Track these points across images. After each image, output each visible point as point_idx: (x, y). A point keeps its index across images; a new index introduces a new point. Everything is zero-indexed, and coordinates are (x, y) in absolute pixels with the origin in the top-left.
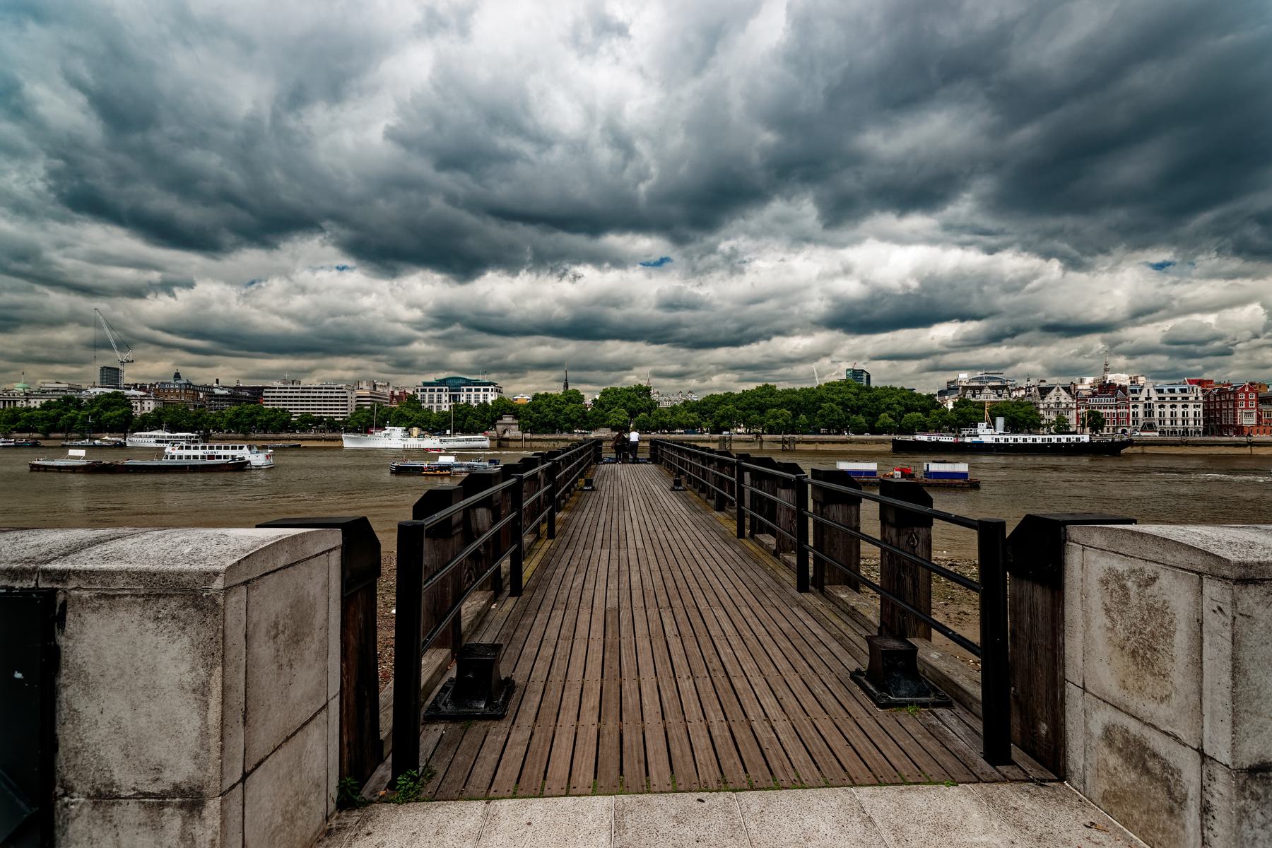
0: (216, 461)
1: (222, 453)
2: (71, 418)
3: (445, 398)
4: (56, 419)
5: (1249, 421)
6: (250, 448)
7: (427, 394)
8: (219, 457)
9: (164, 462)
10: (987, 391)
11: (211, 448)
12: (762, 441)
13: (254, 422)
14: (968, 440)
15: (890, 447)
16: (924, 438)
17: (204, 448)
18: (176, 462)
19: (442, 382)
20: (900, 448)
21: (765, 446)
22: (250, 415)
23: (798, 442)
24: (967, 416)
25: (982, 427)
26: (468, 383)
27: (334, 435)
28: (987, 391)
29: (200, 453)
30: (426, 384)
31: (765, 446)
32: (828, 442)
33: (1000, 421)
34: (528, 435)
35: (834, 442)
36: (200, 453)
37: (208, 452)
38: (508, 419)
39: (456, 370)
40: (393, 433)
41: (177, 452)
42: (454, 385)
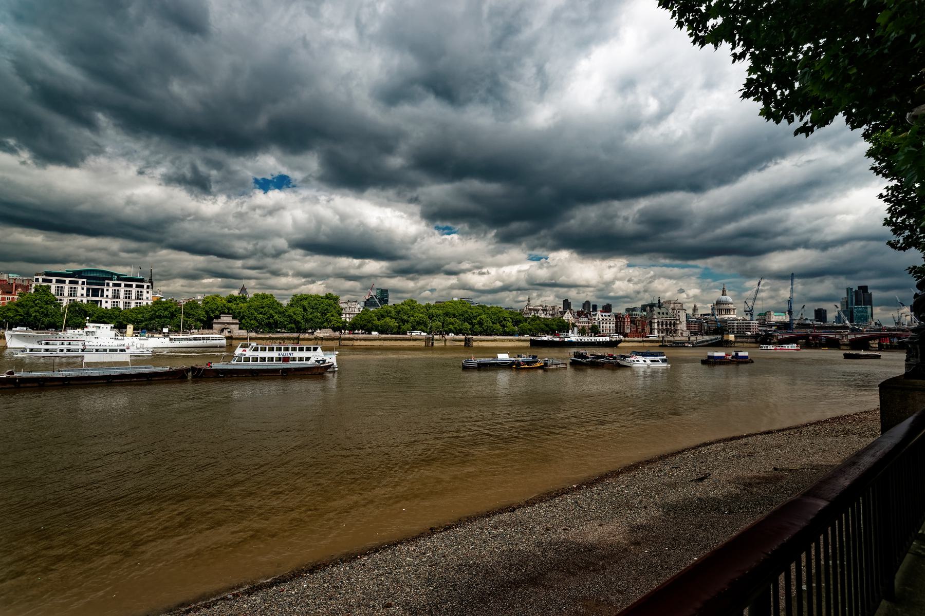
0: (291, 365)
1: (297, 354)
5: (628, 331)
6: (324, 350)
8: (294, 359)
9: (234, 365)
10: (540, 312)
11: (287, 349)
14: (566, 340)
15: (528, 344)
16: (546, 339)
17: (279, 349)
18: (251, 365)
19: (78, 274)
20: (534, 344)
24: (565, 328)
25: (570, 334)
26: (110, 276)
28: (540, 312)
29: (275, 354)
30: (47, 274)
31: (448, 344)
33: (576, 329)
34: (253, 334)
35: (488, 341)
36: (275, 354)
37: (283, 354)
38: (226, 319)
39: (80, 262)
40: (98, 332)
41: (249, 353)
42: (96, 280)
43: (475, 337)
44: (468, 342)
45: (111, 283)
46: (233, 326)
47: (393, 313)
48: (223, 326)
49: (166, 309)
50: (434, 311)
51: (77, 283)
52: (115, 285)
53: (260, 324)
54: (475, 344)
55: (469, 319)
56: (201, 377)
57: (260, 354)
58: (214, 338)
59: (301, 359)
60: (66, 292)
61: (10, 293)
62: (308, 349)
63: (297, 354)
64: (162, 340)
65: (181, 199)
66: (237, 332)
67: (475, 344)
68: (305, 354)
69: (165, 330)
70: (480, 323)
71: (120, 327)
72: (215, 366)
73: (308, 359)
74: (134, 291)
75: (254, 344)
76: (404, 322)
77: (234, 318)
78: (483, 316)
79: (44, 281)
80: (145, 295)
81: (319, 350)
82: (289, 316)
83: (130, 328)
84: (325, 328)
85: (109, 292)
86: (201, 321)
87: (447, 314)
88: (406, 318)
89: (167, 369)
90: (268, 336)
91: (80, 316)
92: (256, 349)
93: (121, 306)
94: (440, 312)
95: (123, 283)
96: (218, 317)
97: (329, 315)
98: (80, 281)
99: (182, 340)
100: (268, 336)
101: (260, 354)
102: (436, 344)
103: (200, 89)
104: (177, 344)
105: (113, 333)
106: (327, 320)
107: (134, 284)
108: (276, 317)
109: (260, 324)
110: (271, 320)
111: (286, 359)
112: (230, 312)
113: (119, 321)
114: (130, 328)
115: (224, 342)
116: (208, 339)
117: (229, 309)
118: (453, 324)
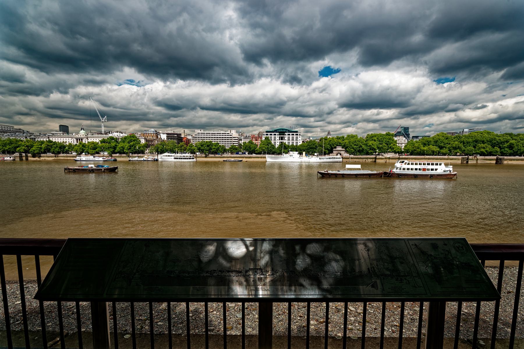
0: (427, 172)
2: (122, 147)
3: (277, 138)
4: (115, 148)
7: (273, 136)
8: (428, 170)
12: (477, 159)
13: (211, 149)
19: (276, 131)
21: (479, 162)
22: (208, 146)
23: (506, 160)
27: (264, 155)
31: (479, 162)
32: (514, 160)
34: (352, 156)
38: (339, 148)
42: (282, 132)
43: (505, 157)
44: (498, 162)
45: (287, 134)
46: (342, 152)
47: (432, 143)
48: (338, 152)
49: (314, 145)
50: (465, 140)
51: (275, 135)
52: (288, 135)
53: (355, 150)
54: (505, 162)
55: (499, 144)
56: (390, 177)
57: (410, 166)
58: (335, 157)
59: (432, 170)
60: (273, 139)
61: (257, 140)
62: (437, 164)
63: (430, 167)
64: (316, 158)
65: (289, 91)
66: (346, 155)
67: (505, 162)
68: (434, 167)
69: (316, 154)
70: (511, 147)
71: (301, 154)
72: (330, 172)
73: (436, 170)
74: (295, 136)
75: (406, 161)
76: (441, 148)
77: (343, 148)
78: (513, 141)
79: (266, 135)
80: (299, 139)
81: (443, 165)
82: (370, 146)
83: (304, 153)
84: (389, 152)
85: (286, 138)
86: (328, 149)
87: (476, 141)
88: (442, 145)
89: (375, 172)
90: (359, 157)
91: (284, 149)
92: (408, 164)
93: (295, 144)
94: (470, 140)
95: (291, 134)
96: (335, 148)
97: (392, 144)
98: (277, 134)
99: (323, 159)
100: (359, 157)
101: (410, 166)
102: (470, 162)
103: (297, 29)
104: (322, 161)
105: (299, 155)
106: (390, 147)
107: (295, 134)
108: (363, 146)
109: (355, 150)
110: (361, 149)
111: (424, 170)
112: (340, 145)
113: (300, 150)
114: (304, 153)
115: (341, 160)
116: (335, 158)
117: (340, 143)
118: (484, 148)
